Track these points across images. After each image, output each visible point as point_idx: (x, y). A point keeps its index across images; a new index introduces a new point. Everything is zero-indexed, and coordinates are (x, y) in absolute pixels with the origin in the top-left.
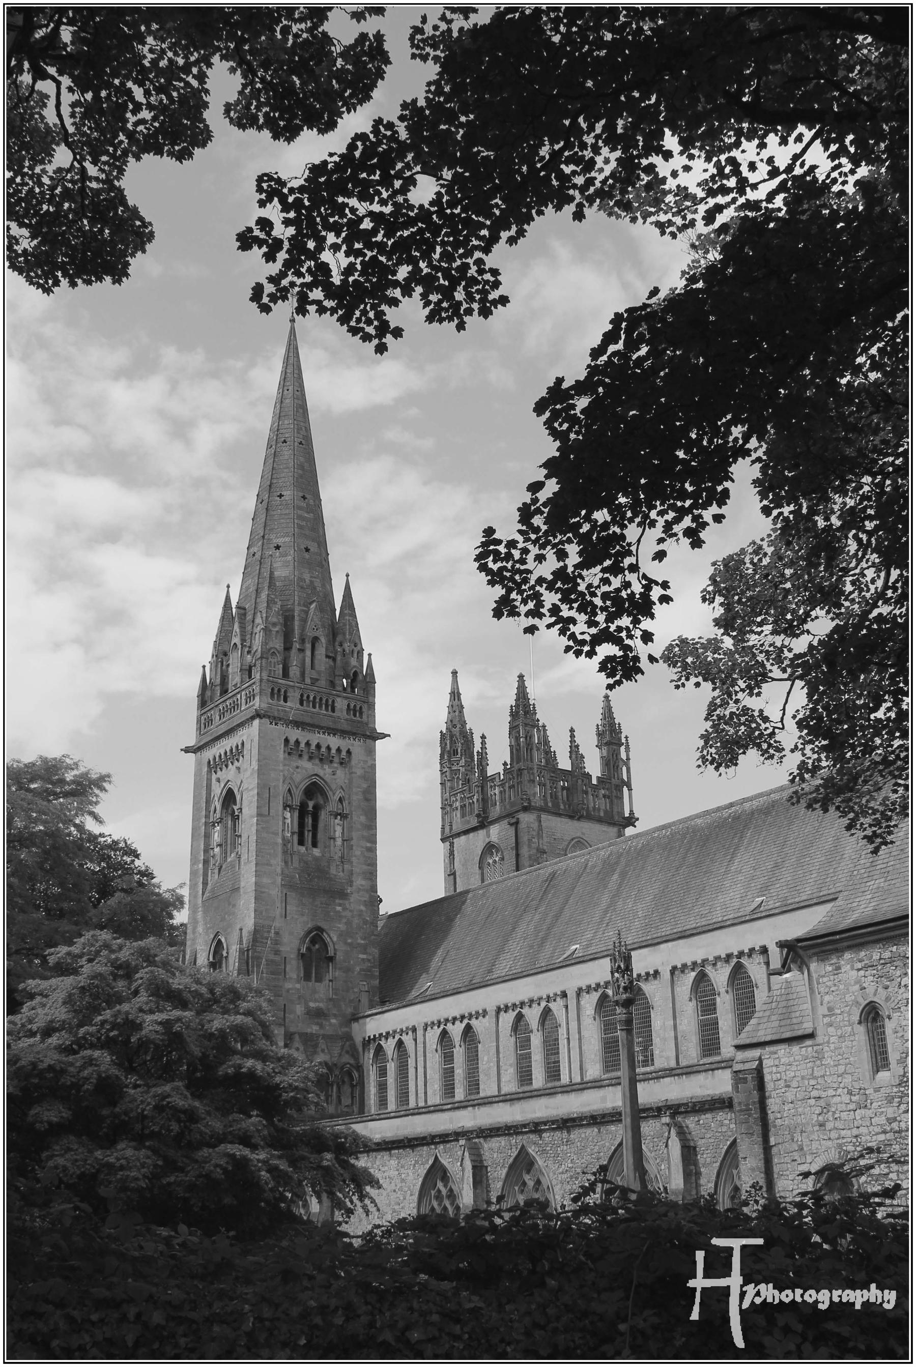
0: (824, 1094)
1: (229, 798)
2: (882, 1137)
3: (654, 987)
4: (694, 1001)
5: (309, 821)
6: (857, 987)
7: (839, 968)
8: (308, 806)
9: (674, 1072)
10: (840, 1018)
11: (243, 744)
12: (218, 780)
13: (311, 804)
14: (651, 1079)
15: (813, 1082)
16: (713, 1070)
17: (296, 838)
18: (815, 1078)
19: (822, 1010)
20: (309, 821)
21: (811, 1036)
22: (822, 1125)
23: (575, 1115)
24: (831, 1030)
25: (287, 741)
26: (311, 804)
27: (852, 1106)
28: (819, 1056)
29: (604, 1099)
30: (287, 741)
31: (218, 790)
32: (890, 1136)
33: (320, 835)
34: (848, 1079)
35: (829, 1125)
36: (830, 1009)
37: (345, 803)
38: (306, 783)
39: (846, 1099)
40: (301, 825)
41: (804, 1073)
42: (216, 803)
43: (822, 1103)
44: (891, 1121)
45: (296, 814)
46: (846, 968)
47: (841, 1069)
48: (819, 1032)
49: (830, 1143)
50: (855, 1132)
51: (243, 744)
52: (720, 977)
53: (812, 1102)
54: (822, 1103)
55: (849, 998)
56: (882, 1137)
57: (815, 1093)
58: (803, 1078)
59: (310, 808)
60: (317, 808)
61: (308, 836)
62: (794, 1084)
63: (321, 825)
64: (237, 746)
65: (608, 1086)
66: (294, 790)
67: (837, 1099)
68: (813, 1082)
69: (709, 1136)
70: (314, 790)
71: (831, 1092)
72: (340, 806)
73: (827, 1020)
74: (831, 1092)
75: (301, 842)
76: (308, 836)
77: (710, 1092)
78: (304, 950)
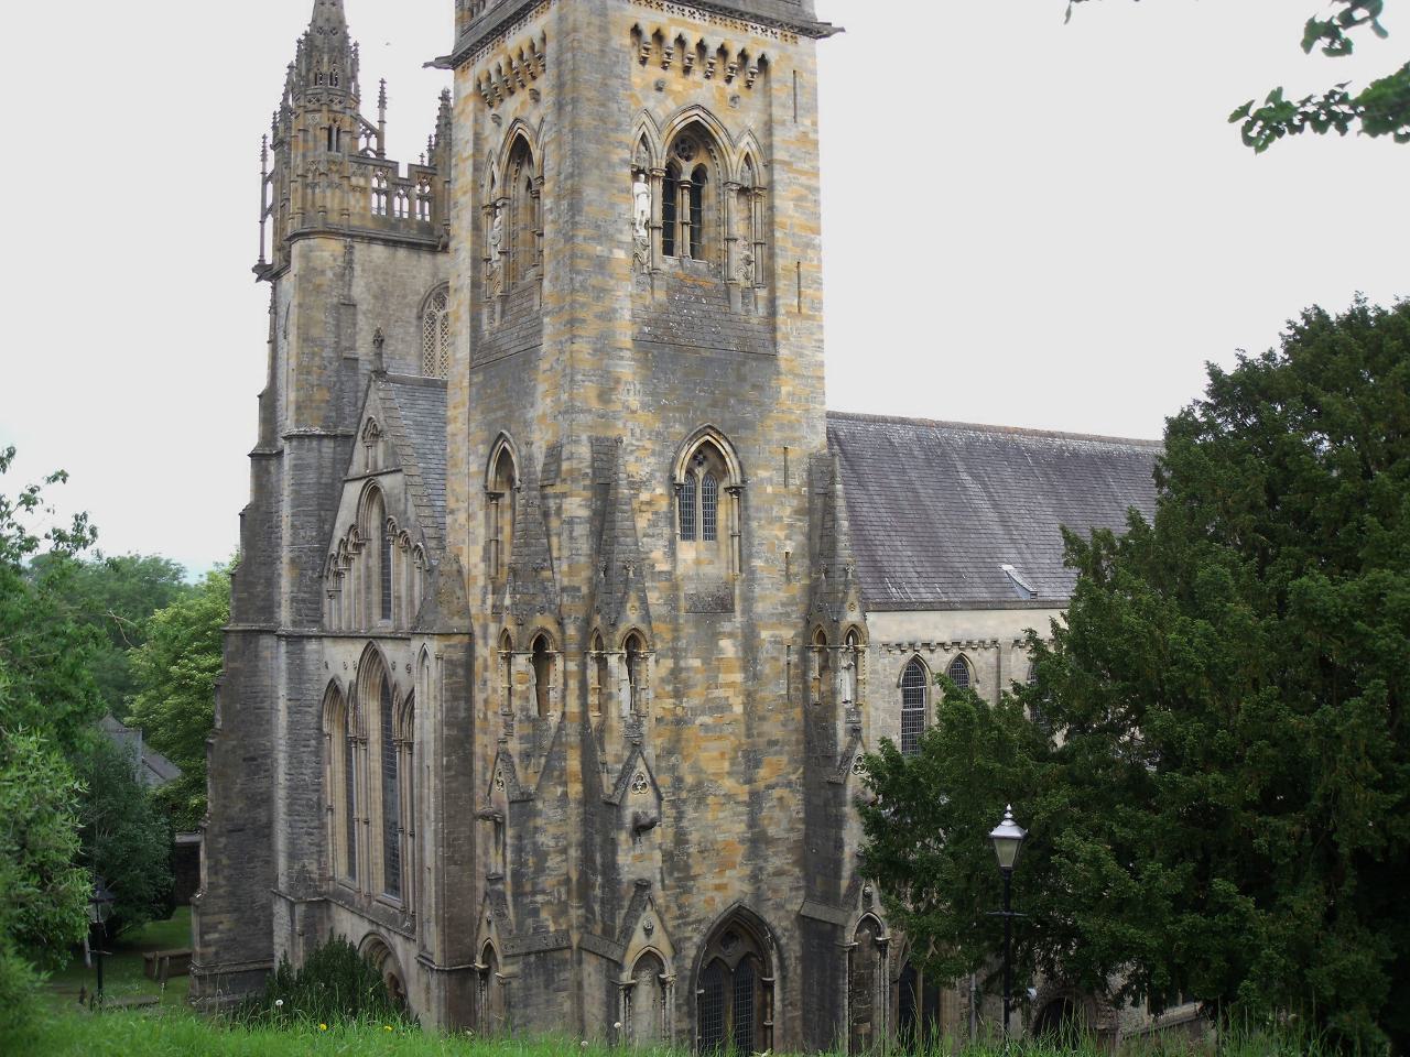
1: (520, 150)
5: (684, 201)
8: (680, 172)
11: (544, 40)
12: (497, 119)
13: (687, 169)
17: (658, 237)
20: (684, 201)
25: (636, 31)
26: (687, 169)
30: (636, 31)
31: (496, 140)
33: (709, 232)
37: (758, 163)
38: (679, 123)
40: (669, 212)
42: (495, 167)
45: (658, 187)
51: (544, 40)
59: (686, 177)
60: (699, 174)
61: (683, 236)
63: (708, 215)
64: (532, 47)
66: (654, 139)
70: (695, 137)
72: (748, 175)
75: (668, 249)
76: (683, 236)
78: (681, 476)
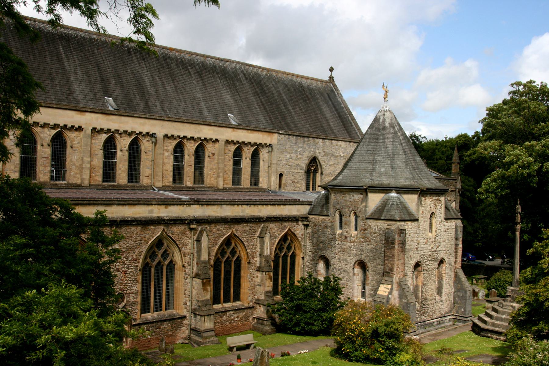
0: (418, 239)
2: (429, 253)
3: (75, 135)
4: (102, 152)
6: (429, 207)
7: (426, 199)
9: (200, 203)
10: (425, 215)
14: (185, 204)
15: (416, 235)
16: (221, 205)
18: (417, 234)
19: (421, 212)
21: (418, 220)
22: (417, 249)
23: (130, 219)
24: (422, 219)
27: (424, 243)
28: (418, 227)
29: (151, 212)
32: (431, 253)
34: (424, 235)
35: (419, 249)
36: (423, 212)
39: (423, 241)
41: (415, 232)
43: (418, 242)
44: (432, 248)
46: (427, 200)
47: (423, 232)
48: (420, 219)
49: (418, 255)
50: (424, 251)
52: (123, 143)
53: (415, 241)
54: (418, 242)
55: (428, 209)
56: (429, 253)
57: (416, 239)
58: (414, 233)
62: (411, 235)
65: (155, 204)
67: (421, 241)
68: (416, 235)
69: (211, 235)
71: (420, 239)
73: (422, 215)
74: (420, 239)
77: (219, 215)
